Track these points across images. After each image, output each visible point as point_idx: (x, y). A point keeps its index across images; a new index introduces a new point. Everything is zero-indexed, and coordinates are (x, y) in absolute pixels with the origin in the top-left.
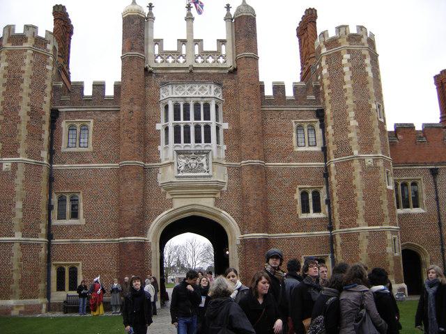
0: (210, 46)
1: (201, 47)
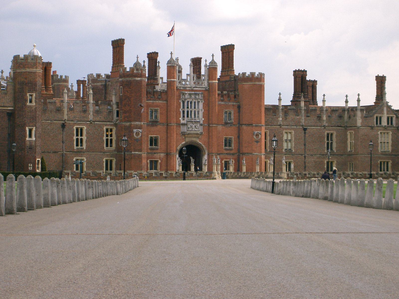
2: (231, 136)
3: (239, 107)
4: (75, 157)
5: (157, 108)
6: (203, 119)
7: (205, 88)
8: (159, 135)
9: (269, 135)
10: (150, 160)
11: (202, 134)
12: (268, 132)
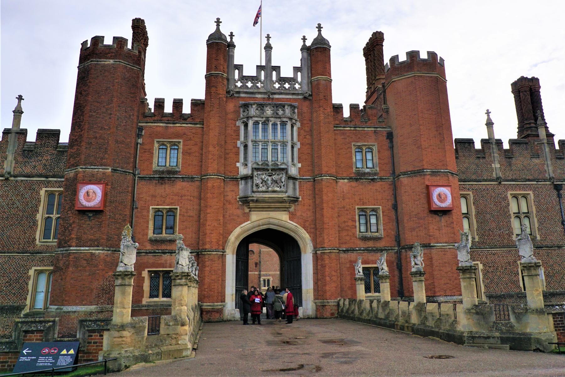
0: (287, 72)
1: (278, 73)
2: (374, 205)
3: (390, 136)
5: (177, 140)
6: (300, 165)
7: (301, 94)
8: (178, 205)
9: (474, 203)
10: (149, 271)
11: (297, 201)
12: (472, 195)
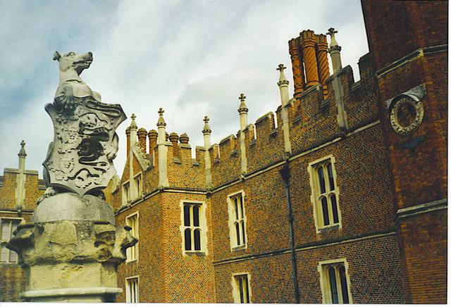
4: (321, 259)
